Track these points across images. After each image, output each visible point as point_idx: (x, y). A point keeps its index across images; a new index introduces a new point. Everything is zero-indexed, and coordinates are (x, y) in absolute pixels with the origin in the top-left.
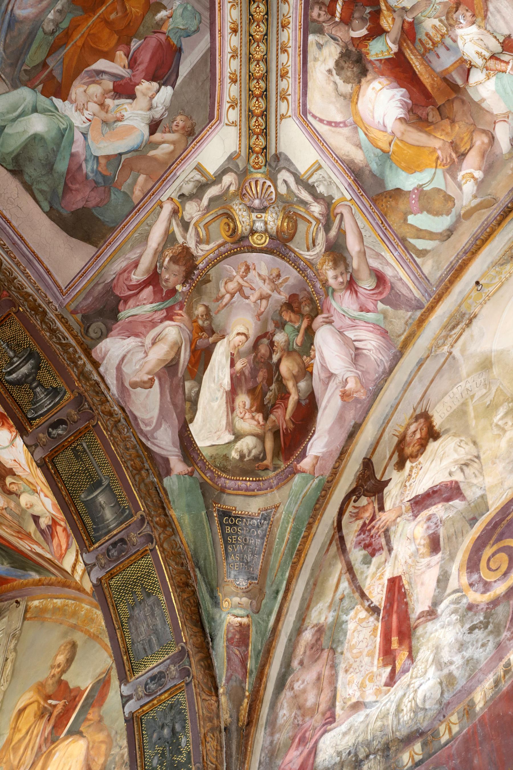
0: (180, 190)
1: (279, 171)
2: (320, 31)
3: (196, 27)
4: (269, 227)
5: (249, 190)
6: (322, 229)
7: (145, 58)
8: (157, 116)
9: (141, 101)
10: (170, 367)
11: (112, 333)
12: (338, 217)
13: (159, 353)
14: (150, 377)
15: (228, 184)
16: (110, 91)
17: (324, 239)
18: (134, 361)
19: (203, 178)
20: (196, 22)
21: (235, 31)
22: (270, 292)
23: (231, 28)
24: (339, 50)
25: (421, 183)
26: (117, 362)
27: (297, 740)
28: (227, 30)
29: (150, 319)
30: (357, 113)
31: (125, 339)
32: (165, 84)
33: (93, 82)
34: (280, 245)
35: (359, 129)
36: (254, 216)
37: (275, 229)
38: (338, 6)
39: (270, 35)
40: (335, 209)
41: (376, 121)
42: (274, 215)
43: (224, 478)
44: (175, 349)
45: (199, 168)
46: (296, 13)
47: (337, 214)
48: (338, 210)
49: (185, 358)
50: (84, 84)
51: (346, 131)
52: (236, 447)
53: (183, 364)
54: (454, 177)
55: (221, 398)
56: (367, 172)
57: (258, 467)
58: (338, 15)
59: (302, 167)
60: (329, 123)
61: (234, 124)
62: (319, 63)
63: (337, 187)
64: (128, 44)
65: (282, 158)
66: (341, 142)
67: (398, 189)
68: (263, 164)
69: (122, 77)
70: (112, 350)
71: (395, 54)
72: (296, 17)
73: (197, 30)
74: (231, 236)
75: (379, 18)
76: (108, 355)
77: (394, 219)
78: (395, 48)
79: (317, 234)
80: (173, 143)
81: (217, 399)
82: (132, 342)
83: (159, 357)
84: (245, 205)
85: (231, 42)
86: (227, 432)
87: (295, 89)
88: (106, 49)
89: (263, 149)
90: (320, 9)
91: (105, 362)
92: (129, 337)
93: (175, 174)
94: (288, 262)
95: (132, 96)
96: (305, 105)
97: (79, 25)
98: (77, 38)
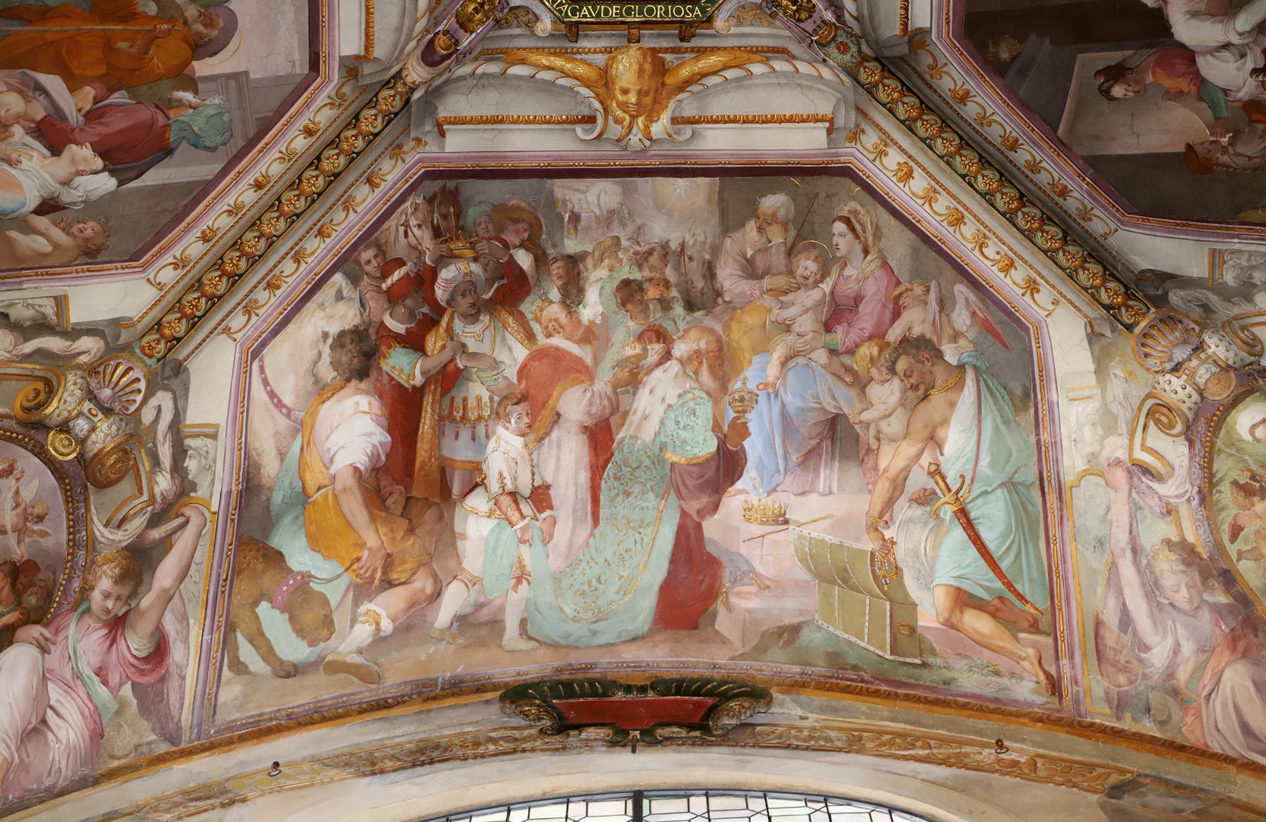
0: (8, 306)
1: (166, 388)
2: (355, 280)
3: (213, 145)
4: (93, 437)
5: (109, 371)
6: (147, 515)
7: (117, 123)
8: (65, 199)
9: (61, 166)
12: (181, 520)
15: (83, 348)
16: (32, 121)
17: (139, 531)
19: (54, 318)
20: (219, 139)
21: (258, 186)
22: (9, 528)
23: (256, 180)
24: (357, 321)
25: (313, 573)
28: (250, 179)
30: (314, 413)
32: (113, 173)
33: (21, 93)
34: (82, 478)
35: (300, 436)
36: (87, 406)
37: (98, 446)
38: (397, 273)
39: (300, 221)
40: (186, 505)
41: (328, 445)
42: (114, 428)
45: (61, 302)
46: (346, 234)
47: (183, 515)
48: (188, 511)
50: (7, 84)
51: (283, 423)
54: (357, 603)
56: (264, 498)
58: (389, 282)
59: (195, 415)
60: (272, 395)
61: (160, 286)
62: (321, 314)
63: (213, 481)
64: (111, 90)
65: (183, 376)
66: (266, 429)
67: (280, 554)
68: (159, 356)
69: (64, 118)
71: (414, 387)
72: (341, 239)
73: (212, 149)
74: (24, 409)
75: (429, 330)
77: (244, 588)
78: (418, 380)
79: (135, 515)
80: (56, 246)
84: (88, 383)
85: (243, 194)
87: (270, 315)
88: (76, 72)
89: (175, 339)
90: (376, 256)
93: (21, 283)
94: (69, 514)
95: (56, 151)
96: (263, 345)
97: (68, 17)
98: (53, 29)
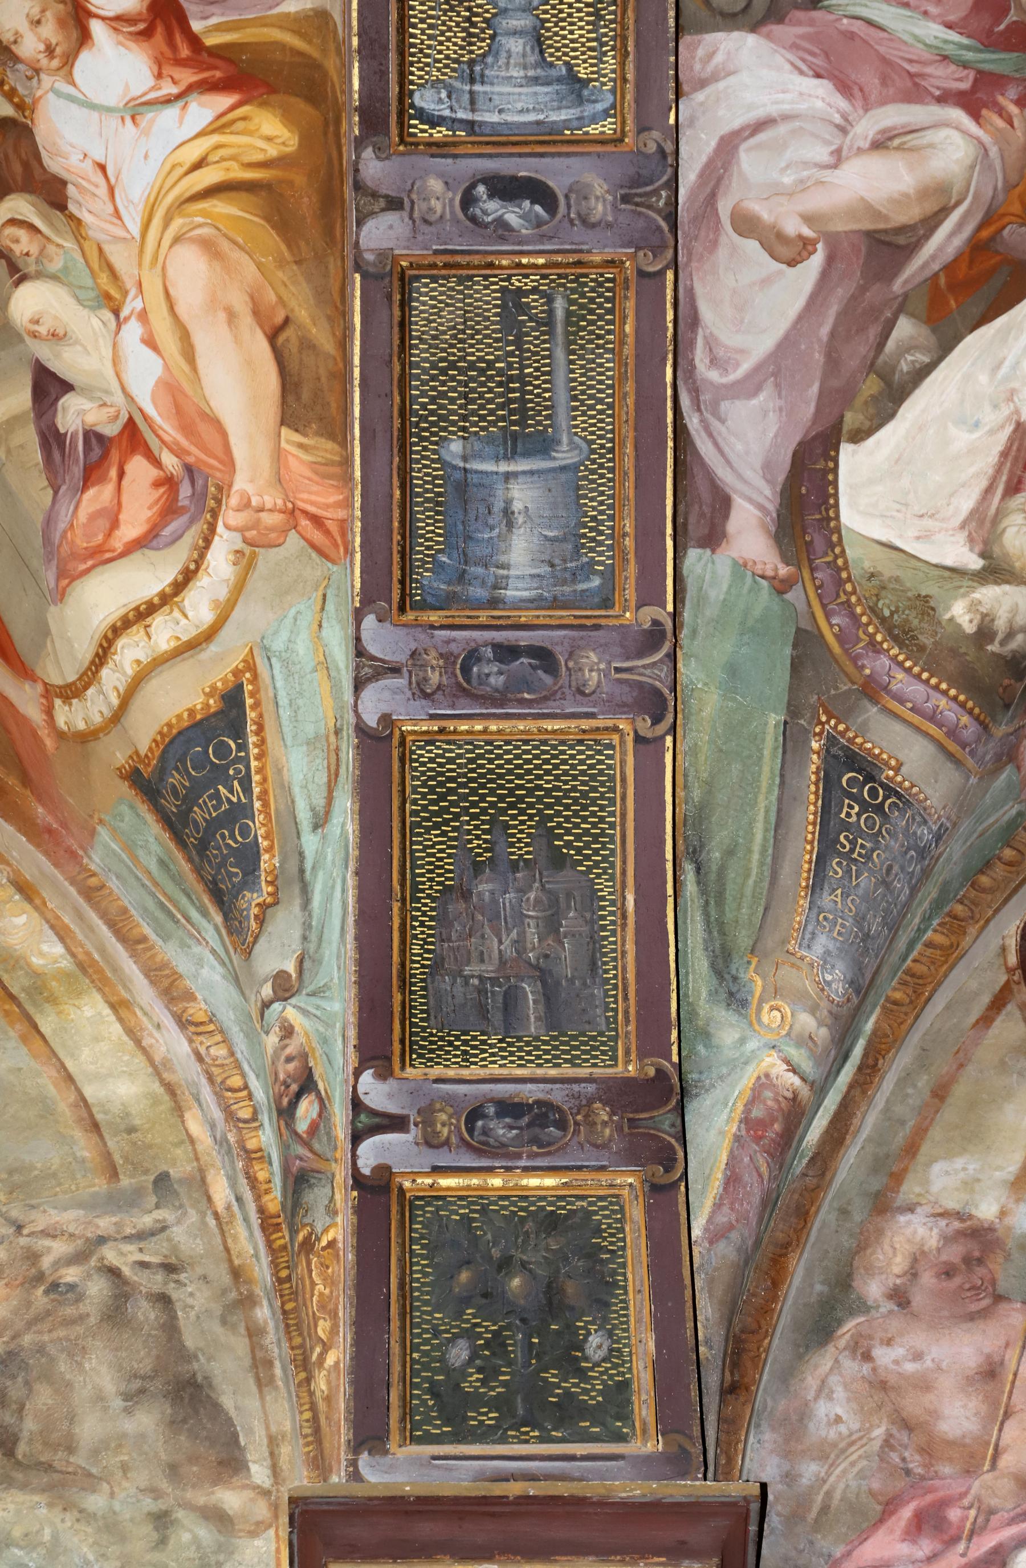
10: (883, 246)
11: (777, 29)
13: (876, 184)
14: (807, 232)
18: (789, 154)
26: (736, 124)
27: (907, 1512)
29: (913, 69)
31: (801, 72)
43: (894, 659)
44: (931, 206)
49: (941, 249)
52: (976, 595)
53: (925, 265)
55: (992, 432)
57: (1005, 688)
70: (744, 77)
76: (721, 85)
81: (977, 425)
82: (818, 96)
83: (864, 194)
86: (962, 537)
91: (700, 96)
92: (818, 76)
